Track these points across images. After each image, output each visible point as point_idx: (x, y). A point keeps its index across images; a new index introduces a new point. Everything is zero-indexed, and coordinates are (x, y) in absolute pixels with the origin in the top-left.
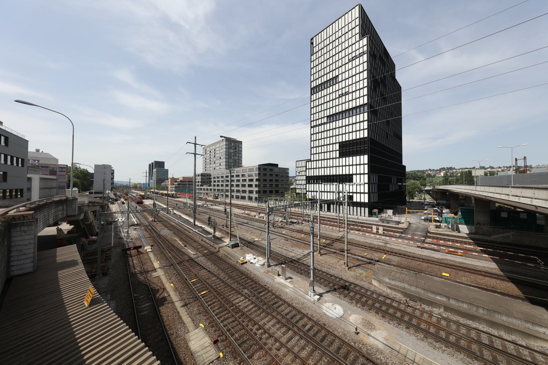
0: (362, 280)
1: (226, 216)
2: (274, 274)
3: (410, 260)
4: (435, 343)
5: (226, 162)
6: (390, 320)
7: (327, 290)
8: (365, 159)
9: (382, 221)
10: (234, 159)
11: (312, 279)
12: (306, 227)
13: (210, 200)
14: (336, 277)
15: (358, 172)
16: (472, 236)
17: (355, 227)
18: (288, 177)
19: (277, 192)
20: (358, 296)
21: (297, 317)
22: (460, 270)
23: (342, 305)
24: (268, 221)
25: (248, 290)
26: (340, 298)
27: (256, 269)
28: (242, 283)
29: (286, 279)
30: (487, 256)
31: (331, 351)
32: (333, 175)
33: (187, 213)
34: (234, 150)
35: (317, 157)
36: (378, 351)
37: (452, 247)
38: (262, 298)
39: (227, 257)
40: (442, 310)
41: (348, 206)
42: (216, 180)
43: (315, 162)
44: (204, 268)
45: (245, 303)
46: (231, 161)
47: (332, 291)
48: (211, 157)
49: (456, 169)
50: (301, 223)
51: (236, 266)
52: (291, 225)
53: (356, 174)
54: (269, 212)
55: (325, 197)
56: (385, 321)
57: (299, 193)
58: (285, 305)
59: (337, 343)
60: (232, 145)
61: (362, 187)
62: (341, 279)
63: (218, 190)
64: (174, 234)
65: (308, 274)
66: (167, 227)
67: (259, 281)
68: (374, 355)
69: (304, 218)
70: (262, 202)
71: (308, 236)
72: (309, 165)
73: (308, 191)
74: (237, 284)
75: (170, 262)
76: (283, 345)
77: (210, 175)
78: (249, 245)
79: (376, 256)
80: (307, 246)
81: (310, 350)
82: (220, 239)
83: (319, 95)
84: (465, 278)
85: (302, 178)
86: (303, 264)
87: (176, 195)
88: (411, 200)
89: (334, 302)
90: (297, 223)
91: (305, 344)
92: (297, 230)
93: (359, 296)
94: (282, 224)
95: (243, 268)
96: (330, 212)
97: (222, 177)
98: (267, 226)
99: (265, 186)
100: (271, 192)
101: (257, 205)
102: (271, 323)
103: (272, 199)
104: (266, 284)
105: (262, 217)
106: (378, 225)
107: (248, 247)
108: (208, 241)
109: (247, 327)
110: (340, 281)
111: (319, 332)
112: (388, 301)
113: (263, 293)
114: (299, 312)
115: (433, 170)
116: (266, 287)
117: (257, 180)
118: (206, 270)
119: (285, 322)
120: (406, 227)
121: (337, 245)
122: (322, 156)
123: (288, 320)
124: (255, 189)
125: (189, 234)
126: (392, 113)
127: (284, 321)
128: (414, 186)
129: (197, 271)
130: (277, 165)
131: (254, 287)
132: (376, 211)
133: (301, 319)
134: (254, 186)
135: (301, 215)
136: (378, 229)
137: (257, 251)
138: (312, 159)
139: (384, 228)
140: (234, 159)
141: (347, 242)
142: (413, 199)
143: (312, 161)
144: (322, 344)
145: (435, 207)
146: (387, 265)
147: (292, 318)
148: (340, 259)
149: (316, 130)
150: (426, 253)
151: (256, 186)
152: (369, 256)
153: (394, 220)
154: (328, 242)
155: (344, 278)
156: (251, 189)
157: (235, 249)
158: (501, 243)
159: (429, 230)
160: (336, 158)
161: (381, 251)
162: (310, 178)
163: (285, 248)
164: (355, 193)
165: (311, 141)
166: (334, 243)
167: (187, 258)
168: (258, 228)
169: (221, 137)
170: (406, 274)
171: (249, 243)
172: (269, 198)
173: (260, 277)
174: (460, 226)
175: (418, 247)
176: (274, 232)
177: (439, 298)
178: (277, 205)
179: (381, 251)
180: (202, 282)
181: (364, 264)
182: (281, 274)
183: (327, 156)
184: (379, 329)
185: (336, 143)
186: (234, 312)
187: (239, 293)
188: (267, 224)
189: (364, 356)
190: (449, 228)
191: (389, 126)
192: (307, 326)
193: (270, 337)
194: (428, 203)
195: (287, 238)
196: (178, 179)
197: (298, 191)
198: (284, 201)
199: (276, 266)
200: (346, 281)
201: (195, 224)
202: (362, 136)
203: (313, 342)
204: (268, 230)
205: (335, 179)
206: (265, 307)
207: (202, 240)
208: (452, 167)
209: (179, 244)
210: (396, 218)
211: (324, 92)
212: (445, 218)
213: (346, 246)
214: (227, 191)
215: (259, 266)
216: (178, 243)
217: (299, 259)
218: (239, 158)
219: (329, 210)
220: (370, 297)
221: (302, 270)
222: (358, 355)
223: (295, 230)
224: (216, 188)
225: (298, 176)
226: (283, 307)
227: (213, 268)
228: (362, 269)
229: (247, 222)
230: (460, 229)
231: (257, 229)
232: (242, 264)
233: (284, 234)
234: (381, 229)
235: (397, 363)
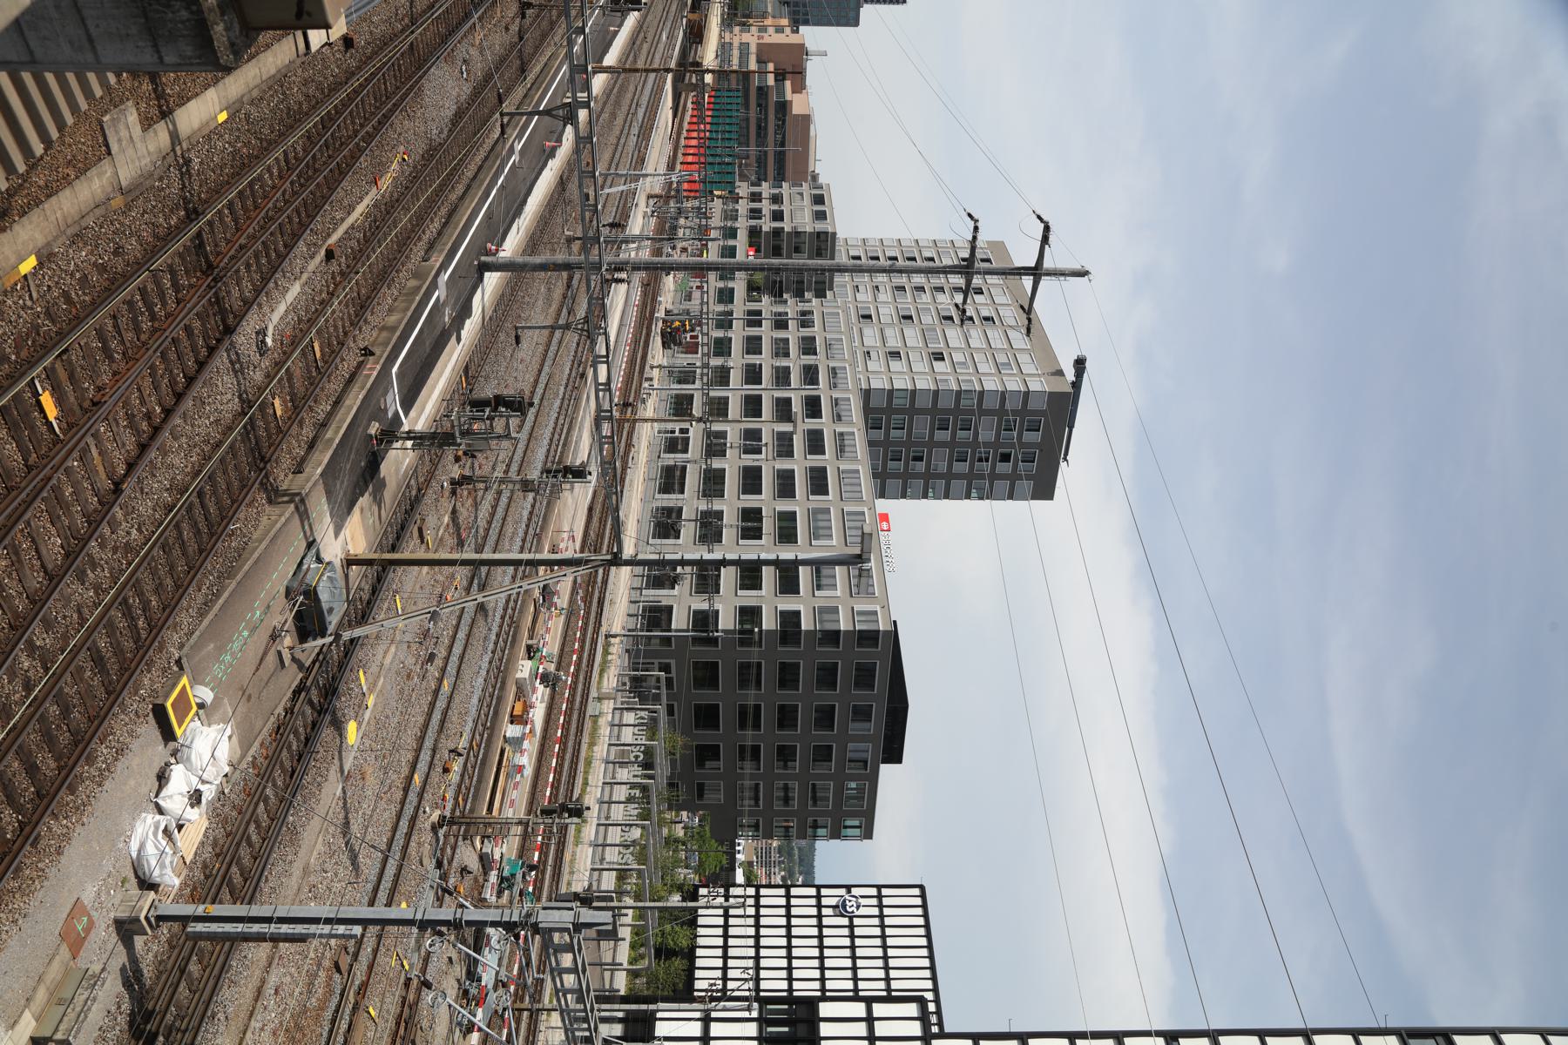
1: (534, 474)
5: (914, 392)
10: (932, 444)
13: (654, 299)
18: (810, 830)
19: (706, 753)
33: (573, 188)
34: (996, 444)
39: (229, 573)
42: (793, 334)
44: (143, 448)
46: (922, 426)
48: (940, 297)
51: (150, 664)
57: (693, 923)
60: (1029, 437)
63: (722, 347)
64: (420, 147)
66: (476, 93)
75: (218, 192)
77: (821, 294)
78: (314, 693)
82: (370, 473)
87: (694, 87)
90: (473, 991)
94: (464, 870)
95: (135, 704)
97: (810, 374)
99: (748, 675)
100: (707, 716)
103: (651, 727)
105: (527, 707)
108: (354, 400)
117: (790, 619)
118: (131, 466)
124: (727, 606)
125: (422, 245)
129: (126, 404)
137: (254, 794)
140: (932, 444)
151: (750, 614)
167: (234, 299)
168: (441, 704)
169: (1080, 364)
171: (330, 691)
176: (409, 836)
180: (29, 468)
195: (356, 956)
196: (800, 87)
198: (643, 827)
199: (127, 984)
201: (485, 268)
207: (367, 352)
209: (350, 209)
214: (710, 528)
216: (361, 199)
218: (940, 476)
224: (738, 334)
225: (819, 897)
227: (145, 508)
231: (432, 705)
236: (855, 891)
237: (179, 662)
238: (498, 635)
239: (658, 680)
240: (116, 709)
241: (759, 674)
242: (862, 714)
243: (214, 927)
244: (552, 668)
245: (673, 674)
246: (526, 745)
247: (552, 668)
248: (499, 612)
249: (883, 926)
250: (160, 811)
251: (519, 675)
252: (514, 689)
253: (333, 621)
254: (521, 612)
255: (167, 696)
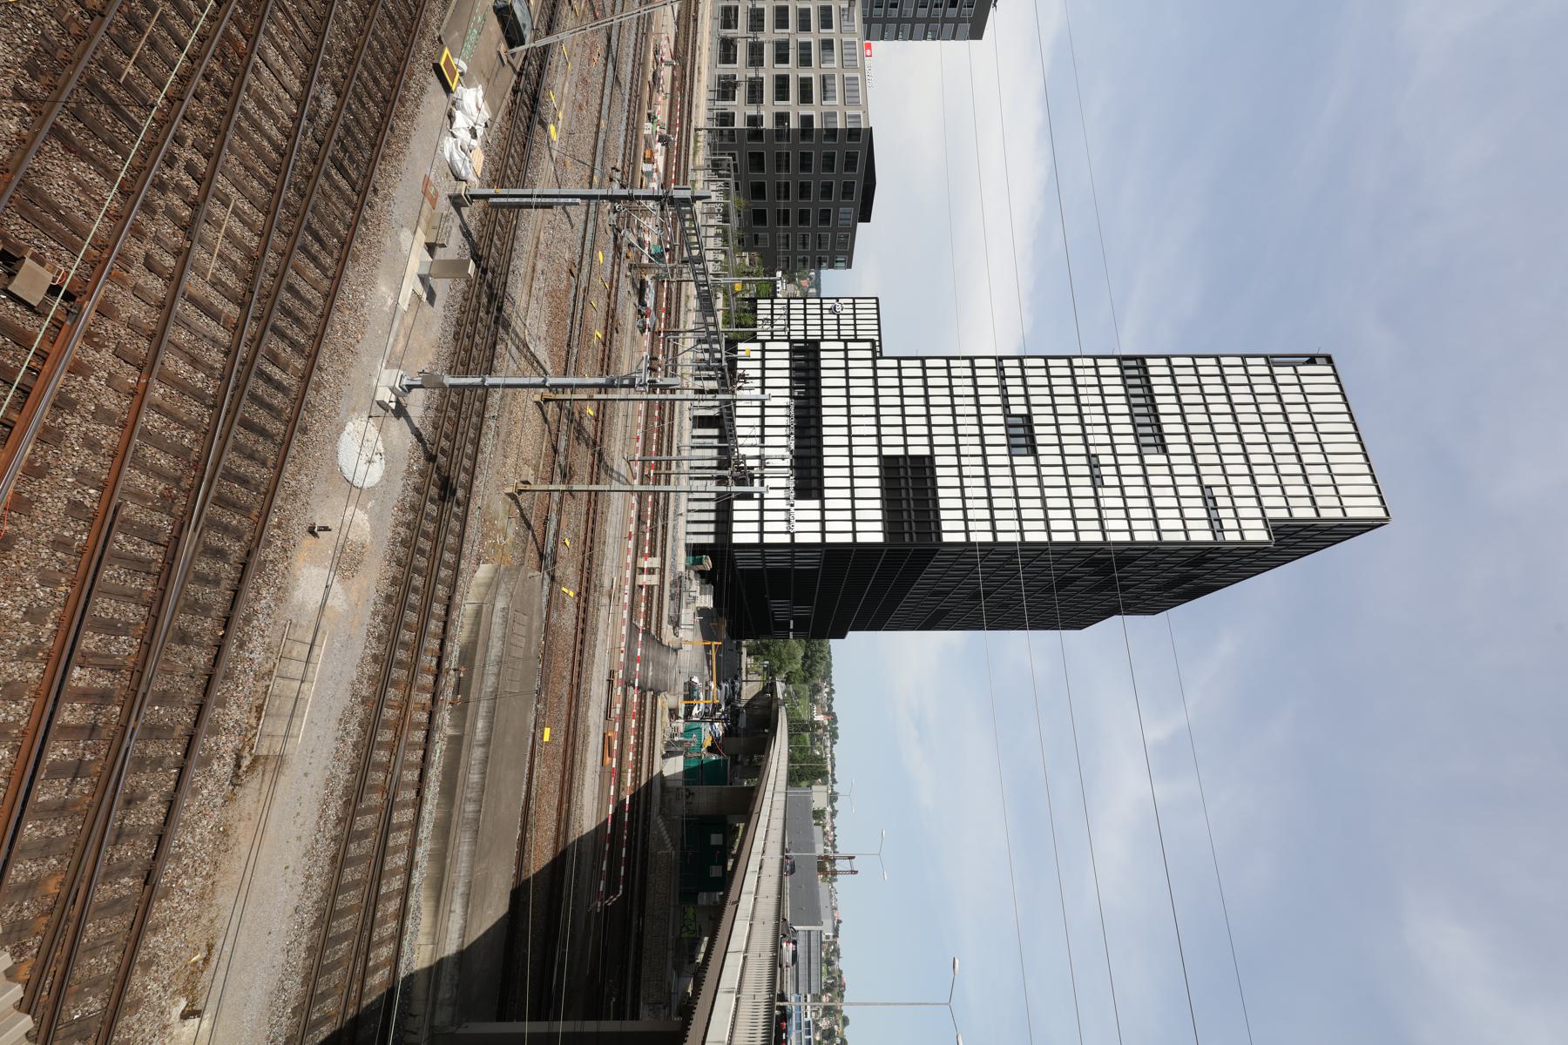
0: (485, 536)
2: (431, 227)
3: (571, 655)
4: (355, 721)
6: (385, 617)
7: (424, 433)
8: (872, 533)
9: (678, 582)
11: (449, 380)
12: (633, 354)
14: (474, 458)
15: (828, 515)
16: (657, 784)
17: (649, 509)
18: (818, 264)
19: (759, 217)
20: (430, 527)
21: (297, 330)
22: (564, 763)
23: (387, 481)
24: (638, 197)
25: (334, 108)
26: (409, 473)
27: (437, 146)
28: (359, 78)
29: (423, 279)
30: (610, 813)
31: (225, 457)
32: (820, 436)
35: (888, 379)
36: (279, 589)
37: (621, 745)
38: (322, 180)
40: (450, 732)
41: (719, 494)
43: (870, 373)
45: (280, 101)
47: (426, 451)
49: (832, 746)
50: (644, 322)
51: (423, 33)
52: (634, 285)
53: (823, 510)
54: (672, 201)
55: (745, 426)
56: (375, 604)
57: (754, 310)
58: (326, 283)
59: (261, 474)
61: (783, 526)
62: (472, 476)
65: (461, 364)
67: (383, 158)
68: (264, 581)
69: (662, 358)
70: (713, 147)
71: (600, 355)
72: (861, 351)
73: (763, 346)
74: (345, 51)
76: (173, 283)
79: (568, 570)
80: (564, 354)
81: (199, 385)
83: (1114, 387)
84: (547, 775)
85: (814, 320)
86: (495, 344)
88: (744, 650)
89: (389, 456)
90: (644, 311)
91: (212, 368)
92: (614, 310)
93: (431, 530)
94: (630, 245)
95: (419, 71)
96: (694, 427)
98: (616, 190)
99: (782, 161)
100: (758, 191)
101: (701, 125)
102: (238, 228)
103: (727, 194)
104: (381, 193)
105: (652, 154)
106: (662, 570)
107: (515, 91)
109: (184, 117)
110: (466, 470)
111: (274, 414)
112: (438, 609)
113: (343, 184)
114: (318, 338)
115: (832, 699)
116: (370, 195)
119: (262, 286)
120: (665, 642)
121: (582, 458)
122: (889, 398)
123: (272, 296)
124: (768, 112)
126: (1006, 606)
127: (264, 280)
128: (784, 656)
130: (866, 217)
131: (355, 139)
132: (708, 564)
133: (294, 344)
134: (781, 106)
135: (673, 331)
136: (651, 571)
138: (880, 363)
139: (656, 589)
141: (596, 492)
142: (749, 655)
143: (875, 363)
144: (235, 426)
145: (727, 705)
146: (544, 600)
147: (288, 312)
148: (536, 469)
149: (988, 378)
150: (597, 689)
151: (782, 118)
152: (562, 550)
153: (683, 611)
154: (589, 426)
155: (476, 483)
156: (768, 90)
157: (494, 26)
158: (645, 852)
159: (662, 694)
160: (880, 446)
161: (584, 584)
162: (811, 356)
163: (540, 265)
164: (762, 505)
165: (948, 359)
166: (587, 445)
170: (528, 648)
171: (535, 99)
172: (731, 180)
173: (404, 165)
174: (680, 759)
175: (612, 673)
177: (480, 724)
178: (703, 233)
179: (584, 584)
181: (536, 540)
182: (436, 257)
183: (890, 417)
184: (347, 590)
185: (931, 445)
186: (221, 45)
187: (310, 67)
188: (624, 192)
189: (249, 553)
190: (672, 736)
191: (970, 599)
192: (277, 370)
193: (184, 228)
194: (737, 689)
195: (580, 270)
197: (763, 304)
198: (725, 252)
200: (469, 489)
202: (945, 526)
203: (232, 396)
204: (603, 197)
205: (806, 442)
206: (289, 194)
208: (837, 737)
210: (688, 616)
211: (1118, 406)
212: (700, 728)
213: (585, 487)
215: (447, 155)
217: (507, 325)
218: (907, 21)
219: (701, 422)
220: (437, 562)
221: (471, 337)
222: (247, 537)
223: (616, 302)
225: (821, 304)
226: (314, 273)
228: (517, 534)
229: (621, 77)
230: (672, 760)
231: (597, 133)
232: (437, 68)
233: (592, 256)
234: (654, 580)
235: (267, 640)
236: (841, 301)
237: (439, 39)
238: (629, 101)
239: (729, 165)
240: (411, 59)
241: (788, 162)
242: (847, 191)
243: (503, 200)
244: (665, 132)
245: (737, 161)
246: (655, 175)
247: (665, 132)
248: (628, 85)
249: (855, 319)
250: (454, 136)
251: (646, 132)
252: (644, 142)
253: (528, 34)
254: (641, 89)
255: (440, 59)
